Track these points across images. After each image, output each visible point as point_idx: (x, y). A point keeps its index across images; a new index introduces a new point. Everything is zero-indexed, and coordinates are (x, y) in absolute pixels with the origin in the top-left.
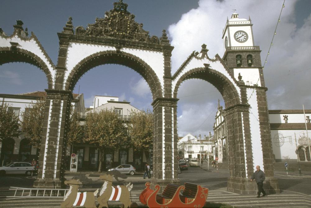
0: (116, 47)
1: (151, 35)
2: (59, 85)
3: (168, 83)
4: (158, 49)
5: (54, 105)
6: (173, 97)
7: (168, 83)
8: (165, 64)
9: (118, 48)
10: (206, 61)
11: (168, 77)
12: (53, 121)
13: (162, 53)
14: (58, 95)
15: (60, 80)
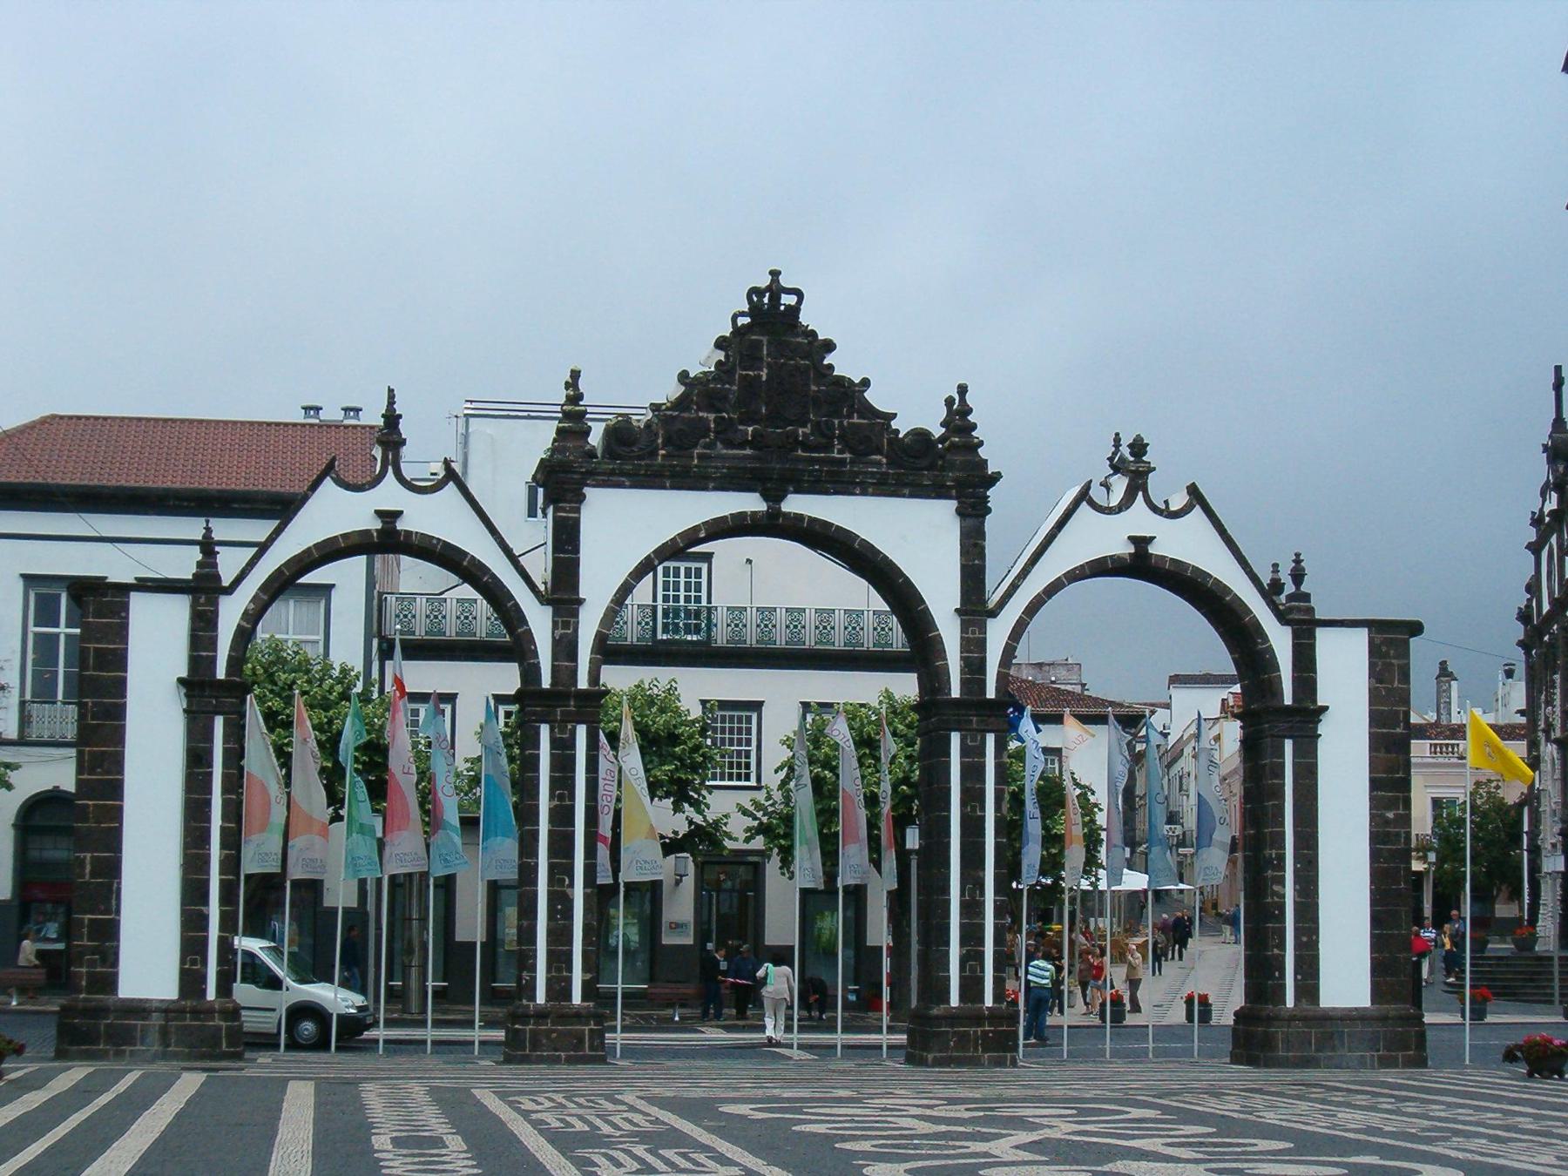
0: (766, 497)
1: (902, 426)
2: (566, 666)
3: (973, 633)
4: (937, 491)
5: (555, 743)
6: (991, 693)
7: (973, 633)
8: (964, 552)
9: (774, 496)
10: (1139, 520)
11: (975, 609)
12: (556, 803)
13: (953, 504)
14: (569, 706)
15: (565, 648)
